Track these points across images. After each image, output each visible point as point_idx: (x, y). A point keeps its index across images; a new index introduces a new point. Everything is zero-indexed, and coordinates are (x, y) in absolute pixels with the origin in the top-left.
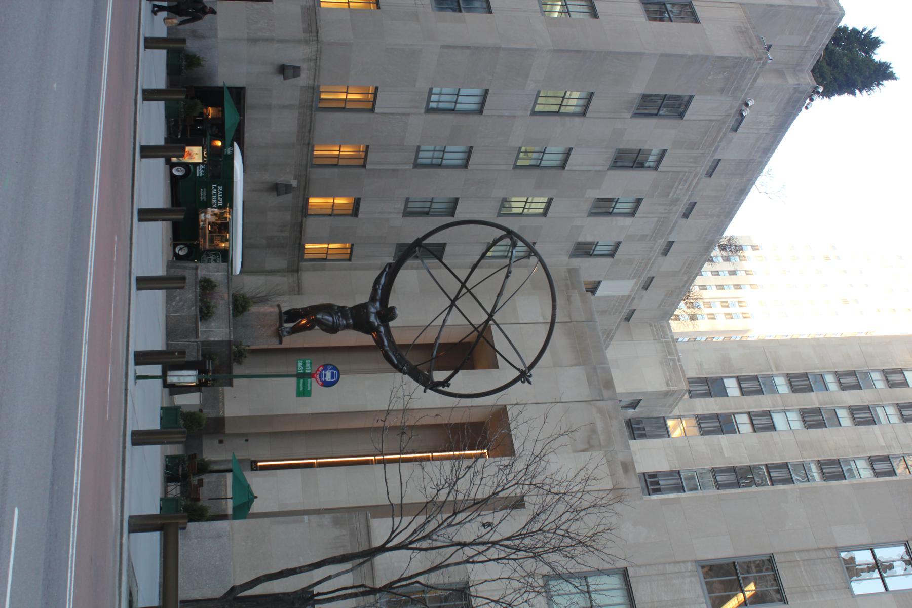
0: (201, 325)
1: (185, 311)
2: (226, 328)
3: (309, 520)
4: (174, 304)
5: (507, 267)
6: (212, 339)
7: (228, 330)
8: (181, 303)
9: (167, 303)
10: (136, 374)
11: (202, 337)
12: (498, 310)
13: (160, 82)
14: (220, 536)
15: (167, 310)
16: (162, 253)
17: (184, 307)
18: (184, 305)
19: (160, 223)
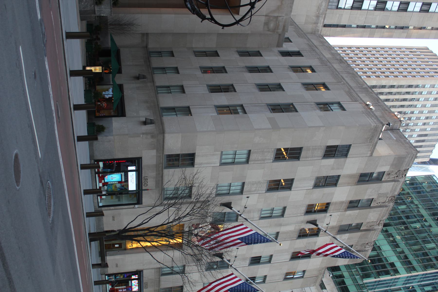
0: (97, 7)
1: (89, 8)
2: (109, 9)
3: (142, 136)
4: (83, 3)
5: (252, 14)
6: (102, 15)
7: (110, 10)
8: (86, 3)
9: (79, 3)
10: (73, 104)
11: (97, 14)
12: (244, 20)
13: (82, 101)
14: (110, 141)
15: (80, 7)
16: (78, 24)
17: (88, 5)
18: (88, 4)
19: (85, 110)
